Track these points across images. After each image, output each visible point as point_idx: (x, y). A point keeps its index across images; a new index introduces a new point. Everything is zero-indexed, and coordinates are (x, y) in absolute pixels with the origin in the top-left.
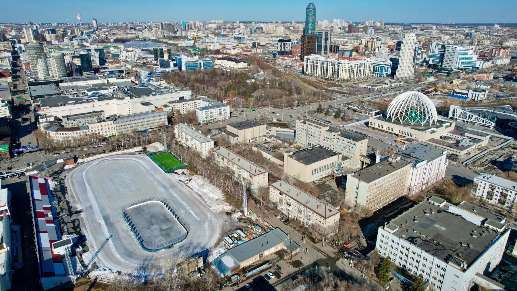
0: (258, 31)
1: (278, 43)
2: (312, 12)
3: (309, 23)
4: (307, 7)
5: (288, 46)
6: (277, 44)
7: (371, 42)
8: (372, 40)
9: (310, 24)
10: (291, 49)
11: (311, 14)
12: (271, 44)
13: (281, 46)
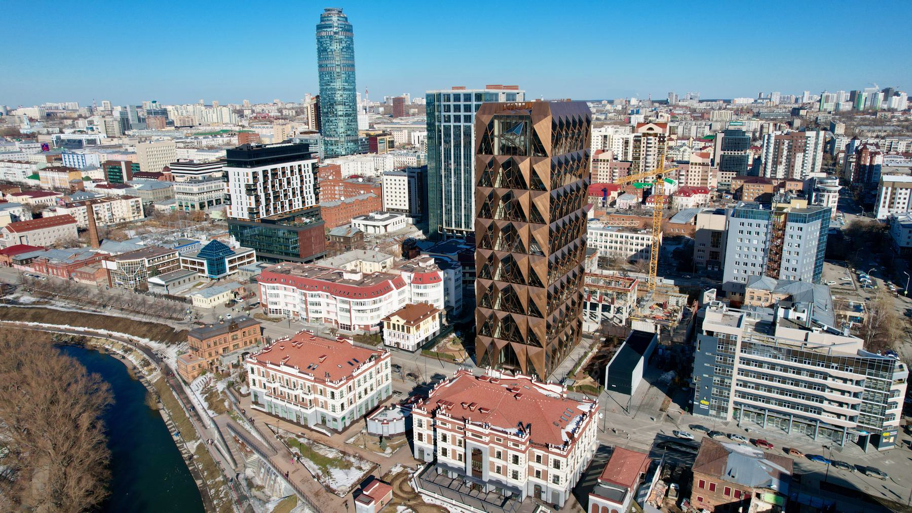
0: (152, 120)
1: (232, 171)
2: (341, 41)
3: (332, 80)
6: (226, 176)
7: (654, 141)
8: (658, 130)
9: (338, 84)
10: (311, 202)
11: (335, 46)
12: (191, 163)
13: (250, 190)
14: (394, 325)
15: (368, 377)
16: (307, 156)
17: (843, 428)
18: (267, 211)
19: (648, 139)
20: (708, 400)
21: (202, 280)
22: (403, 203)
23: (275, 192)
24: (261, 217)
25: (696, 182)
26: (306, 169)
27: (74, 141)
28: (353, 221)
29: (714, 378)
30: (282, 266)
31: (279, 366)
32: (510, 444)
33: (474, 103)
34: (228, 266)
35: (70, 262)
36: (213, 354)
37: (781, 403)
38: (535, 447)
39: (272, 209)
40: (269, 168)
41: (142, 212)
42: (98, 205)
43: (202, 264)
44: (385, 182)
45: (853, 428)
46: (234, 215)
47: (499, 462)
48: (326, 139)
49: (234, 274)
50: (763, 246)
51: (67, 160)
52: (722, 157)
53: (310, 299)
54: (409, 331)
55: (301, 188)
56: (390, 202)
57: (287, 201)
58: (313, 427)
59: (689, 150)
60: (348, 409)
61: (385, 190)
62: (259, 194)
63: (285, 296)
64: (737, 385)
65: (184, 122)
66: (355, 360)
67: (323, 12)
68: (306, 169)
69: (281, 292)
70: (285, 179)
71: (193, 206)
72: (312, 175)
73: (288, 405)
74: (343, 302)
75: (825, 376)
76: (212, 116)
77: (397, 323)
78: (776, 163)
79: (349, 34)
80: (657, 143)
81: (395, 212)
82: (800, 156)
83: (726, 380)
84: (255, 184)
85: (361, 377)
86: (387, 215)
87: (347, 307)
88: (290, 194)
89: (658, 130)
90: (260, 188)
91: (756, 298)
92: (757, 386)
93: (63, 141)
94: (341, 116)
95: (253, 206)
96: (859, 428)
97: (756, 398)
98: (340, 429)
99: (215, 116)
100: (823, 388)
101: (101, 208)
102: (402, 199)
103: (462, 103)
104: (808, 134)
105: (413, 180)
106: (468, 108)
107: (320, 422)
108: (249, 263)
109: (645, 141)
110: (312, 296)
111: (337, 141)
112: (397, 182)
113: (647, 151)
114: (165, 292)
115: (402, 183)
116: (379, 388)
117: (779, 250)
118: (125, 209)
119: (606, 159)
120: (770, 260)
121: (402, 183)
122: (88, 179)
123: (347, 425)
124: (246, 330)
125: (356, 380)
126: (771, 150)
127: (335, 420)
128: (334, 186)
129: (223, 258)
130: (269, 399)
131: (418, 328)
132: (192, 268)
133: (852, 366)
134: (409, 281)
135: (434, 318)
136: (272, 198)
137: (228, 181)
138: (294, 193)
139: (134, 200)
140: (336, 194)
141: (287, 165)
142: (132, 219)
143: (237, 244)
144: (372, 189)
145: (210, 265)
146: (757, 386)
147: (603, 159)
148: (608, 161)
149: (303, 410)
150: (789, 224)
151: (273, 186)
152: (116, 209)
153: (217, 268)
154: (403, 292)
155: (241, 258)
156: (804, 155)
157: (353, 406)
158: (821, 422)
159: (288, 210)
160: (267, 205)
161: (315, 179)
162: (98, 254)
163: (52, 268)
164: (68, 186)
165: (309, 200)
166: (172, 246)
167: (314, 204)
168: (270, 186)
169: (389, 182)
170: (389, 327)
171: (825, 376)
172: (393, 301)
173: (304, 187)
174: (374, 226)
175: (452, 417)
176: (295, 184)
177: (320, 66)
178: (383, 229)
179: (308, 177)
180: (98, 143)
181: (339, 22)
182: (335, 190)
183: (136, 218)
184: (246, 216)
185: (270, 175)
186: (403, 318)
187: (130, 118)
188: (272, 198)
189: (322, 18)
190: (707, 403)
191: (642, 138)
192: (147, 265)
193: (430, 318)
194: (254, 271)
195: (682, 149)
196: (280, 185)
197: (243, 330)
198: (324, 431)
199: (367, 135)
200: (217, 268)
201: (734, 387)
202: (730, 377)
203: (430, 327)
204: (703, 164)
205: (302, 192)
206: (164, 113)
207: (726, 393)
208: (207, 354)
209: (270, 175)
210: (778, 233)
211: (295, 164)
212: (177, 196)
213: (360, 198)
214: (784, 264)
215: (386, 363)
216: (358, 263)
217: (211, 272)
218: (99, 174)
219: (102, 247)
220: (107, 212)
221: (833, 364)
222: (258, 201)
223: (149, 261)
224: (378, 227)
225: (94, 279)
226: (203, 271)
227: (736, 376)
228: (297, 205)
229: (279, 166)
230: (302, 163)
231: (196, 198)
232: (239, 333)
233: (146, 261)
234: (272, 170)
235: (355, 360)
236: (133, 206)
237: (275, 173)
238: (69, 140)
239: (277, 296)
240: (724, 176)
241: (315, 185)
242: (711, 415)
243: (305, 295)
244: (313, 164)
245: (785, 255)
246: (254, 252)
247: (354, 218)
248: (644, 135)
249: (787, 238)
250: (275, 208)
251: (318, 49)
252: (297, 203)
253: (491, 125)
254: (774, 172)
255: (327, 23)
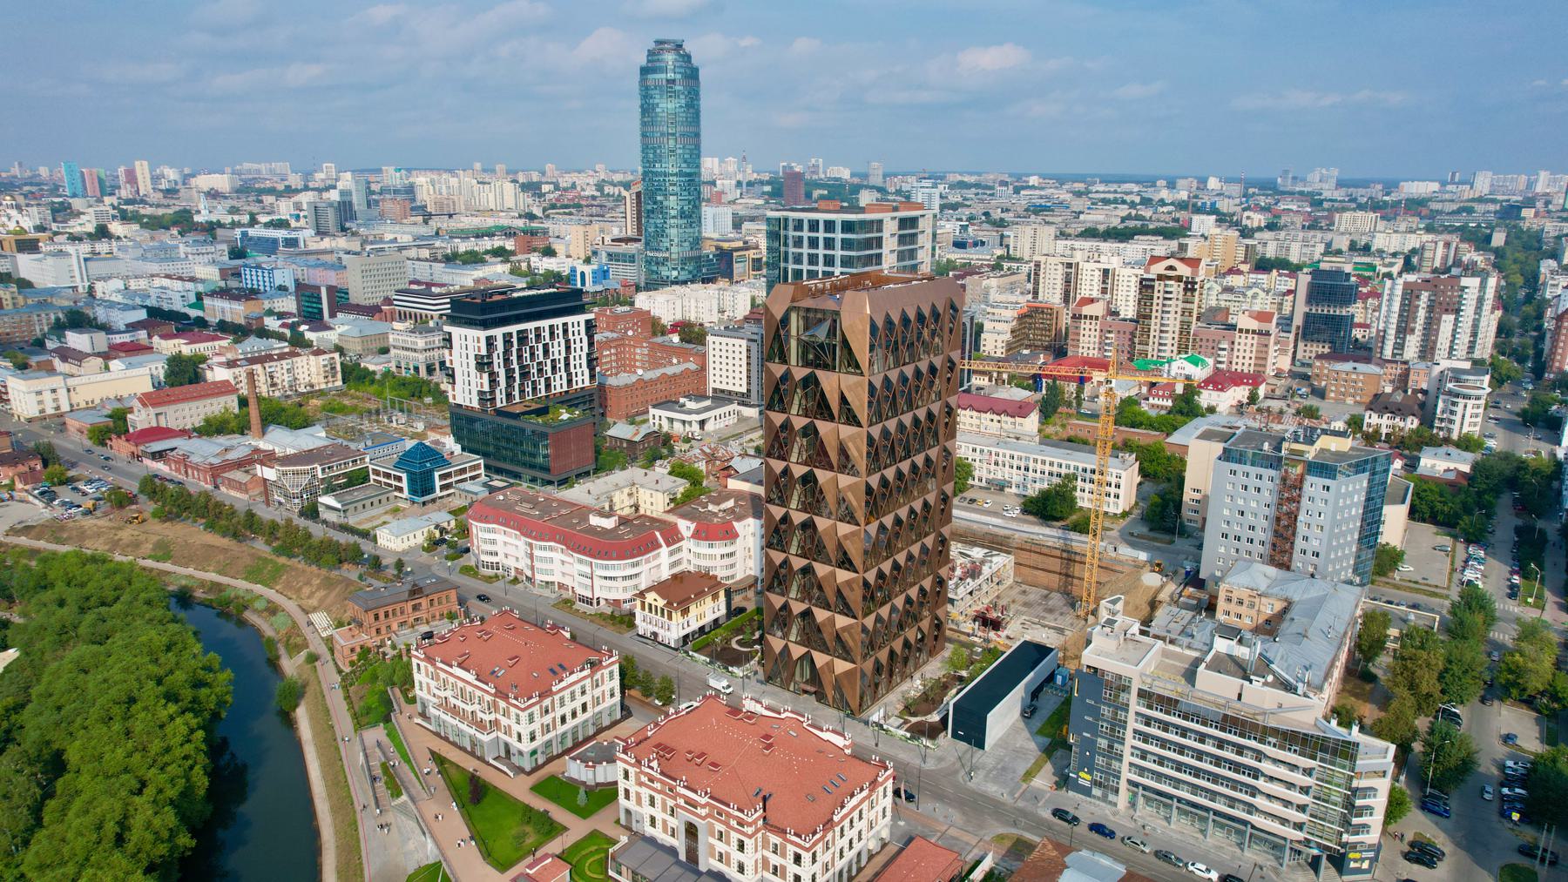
1: (457, 332)
4: (643, 61)
5: (558, 350)
6: (448, 340)
7: (1176, 289)
8: (1184, 270)
10: (582, 380)
13: (483, 364)
14: (650, 605)
15: (578, 693)
16: (580, 310)
17: (1285, 839)
18: (509, 396)
19: (1166, 285)
20: (1089, 772)
21: (402, 504)
22: (737, 382)
23: (522, 367)
24: (499, 405)
25: (1247, 361)
26: (576, 329)
27: (267, 240)
28: (652, 411)
29: (1099, 740)
30: (505, 495)
31: (451, 666)
32: (733, 823)
33: (839, 236)
34: (438, 483)
35: (216, 461)
36: (383, 631)
37: (1195, 789)
38: (770, 831)
39: (516, 393)
40: (513, 329)
41: (339, 376)
42: (274, 364)
43: (399, 479)
44: (711, 346)
45: (1299, 842)
46: (459, 401)
47: (720, 847)
48: (649, 254)
49: (449, 495)
50: (1267, 511)
51: (248, 277)
52: (1307, 316)
53: (537, 553)
54: (670, 618)
55: (567, 359)
56: (717, 378)
57: (542, 380)
58: (492, 761)
59: (1262, 294)
60: (540, 740)
61: (711, 359)
62: (496, 369)
63: (505, 543)
64: (1132, 754)
65: (442, 208)
66: (561, 666)
67: (652, 46)
68: (576, 329)
69: (500, 538)
70: (540, 346)
71: (416, 369)
72: (585, 339)
73: (460, 725)
74: (581, 561)
75: (1259, 756)
76: (488, 198)
77: (654, 603)
78: (1404, 330)
79: (691, 82)
80: (1182, 293)
81: (723, 397)
82: (1448, 320)
83: (1116, 745)
84: (490, 355)
85: (567, 693)
86: (708, 403)
87: (588, 570)
88: (549, 368)
89: (1184, 270)
90: (498, 361)
91: (1235, 600)
92: (1161, 761)
93: (251, 239)
94: (674, 217)
95: (486, 388)
96: (1307, 842)
97: (1159, 776)
98: (528, 768)
99: (491, 197)
100: (1256, 774)
101: (278, 369)
102: (737, 375)
103: (821, 235)
104: (1465, 281)
105: (754, 347)
106: (829, 244)
107: (503, 754)
108: (472, 478)
109: (1161, 288)
110: (541, 548)
111: (666, 259)
112: (730, 348)
113: (1164, 305)
114: (342, 521)
115: (737, 349)
116: (597, 709)
117: (1293, 517)
118: (313, 370)
119: (1094, 314)
120: (1276, 533)
121: (737, 349)
122: (270, 313)
123: (540, 761)
124: (435, 597)
125: (557, 697)
126: (1396, 307)
127: (521, 753)
128: (635, 347)
129: (431, 472)
130: (437, 713)
131: (685, 612)
132: (386, 484)
133: (1297, 745)
134: (689, 534)
135: (715, 597)
136: (517, 375)
137: (451, 347)
138: (554, 368)
139: (327, 356)
140: (636, 360)
141: (544, 324)
142: (323, 386)
143: (457, 449)
144: (692, 355)
145: (411, 481)
146: (1161, 761)
147: (1089, 314)
148: (1097, 318)
149: (479, 735)
150: (1310, 479)
151: (520, 357)
152: (300, 370)
153: (422, 486)
154: (679, 549)
155: (463, 471)
156: (1456, 319)
157: (551, 735)
158: (1253, 827)
159: (543, 393)
160: (509, 385)
161: (591, 344)
162: (257, 450)
163: (192, 467)
164: (242, 321)
165: (580, 378)
166: (361, 446)
167: (587, 383)
168: (514, 358)
169: (717, 346)
170: (643, 608)
171: (1259, 756)
172: (660, 564)
173: (571, 357)
174: (684, 422)
175: (662, 773)
176: (556, 353)
177: (644, 135)
178: (696, 427)
179: (578, 341)
180: (302, 245)
181: (678, 64)
182: (635, 354)
183: (330, 385)
184: (475, 404)
185: (515, 340)
186: (663, 598)
187: (355, 200)
188: (517, 375)
189: (651, 53)
190: (1088, 777)
191: (1157, 283)
192: (320, 476)
193: (709, 599)
194: (476, 494)
195: (1250, 293)
196: (532, 354)
197: (431, 597)
198: (505, 769)
199: (718, 248)
200: (422, 486)
201: (1128, 758)
202: (1122, 741)
203: (709, 610)
204: (1260, 333)
205: (567, 365)
206: (410, 190)
207: (1115, 764)
208: (374, 630)
209: (515, 340)
210: (1290, 492)
211: (558, 321)
212: (393, 351)
213: (670, 371)
214: (1299, 543)
215: (611, 673)
216: (634, 490)
217: (413, 491)
218: (289, 304)
219: (266, 437)
220: (286, 375)
221: (1270, 739)
222: (493, 382)
223: (323, 470)
224: (690, 423)
225: (246, 491)
226: (400, 489)
227: (1130, 740)
228: (559, 385)
229: (530, 326)
230: (569, 319)
231: (421, 357)
232: (424, 602)
233: (319, 469)
234: (519, 332)
235: (561, 666)
236: (325, 366)
237: (523, 337)
238: (259, 239)
239: (493, 542)
240: (1308, 348)
241: (588, 355)
242: (1094, 797)
243: (531, 545)
244: (588, 322)
245: (1301, 529)
246: (482, 461)
247: (654, 406)
248: (1160, 277)
249: (1305, 502)
250: (522, 391)
251: (642, 106)
252: (558, 383)
253: (785, 321)
254: (1400, 346)
255: (658, 64)
